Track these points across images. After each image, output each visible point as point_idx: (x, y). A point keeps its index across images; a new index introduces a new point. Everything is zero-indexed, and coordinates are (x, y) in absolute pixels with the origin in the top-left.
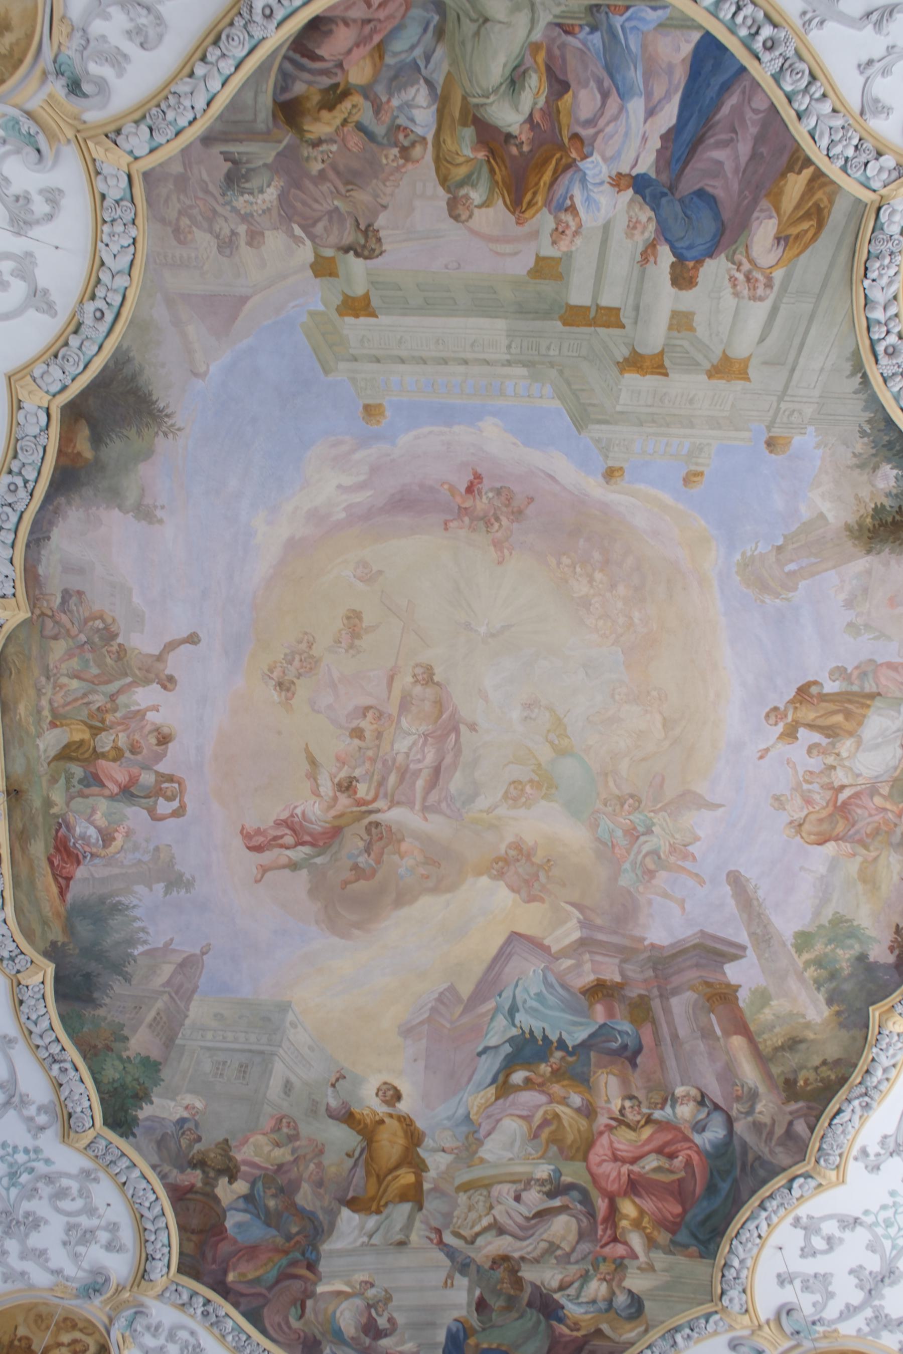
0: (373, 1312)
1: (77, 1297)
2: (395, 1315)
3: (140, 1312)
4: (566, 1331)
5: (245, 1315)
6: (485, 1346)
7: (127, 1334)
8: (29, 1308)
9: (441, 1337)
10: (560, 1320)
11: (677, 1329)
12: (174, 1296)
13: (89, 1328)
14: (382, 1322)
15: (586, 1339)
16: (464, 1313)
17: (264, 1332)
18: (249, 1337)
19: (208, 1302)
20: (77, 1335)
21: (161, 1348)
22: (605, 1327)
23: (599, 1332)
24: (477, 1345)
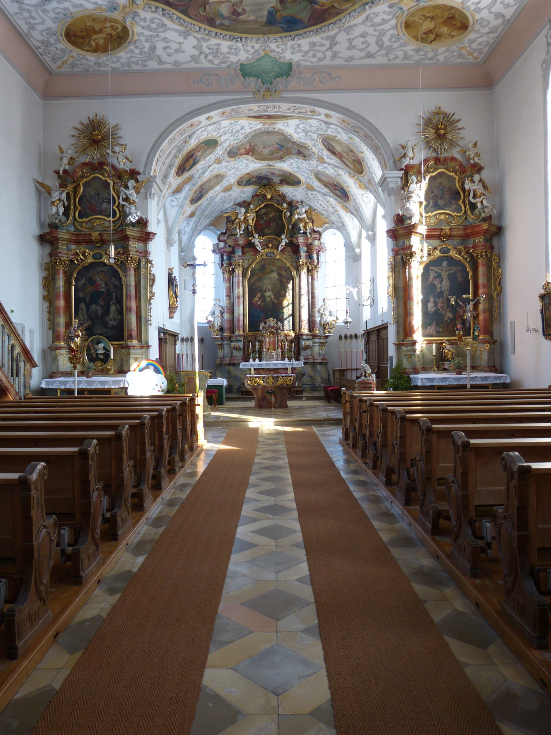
0: (235, 7)
1: (107, 11)
2: (245, 7)
3: (136, 14)
4: (319, 7)
5: (180, 12)
6: (284, 15)
7: (133, 22)
8: (89, 16)
9: (265, 13)
10: (316, 4)
11: (366, 4)
12: (149, 9)
13: (116, 21)
14: (240, 10)
15: (327, 10)
16: (274, 4)
17: (190, 17)
18: (184, 20)
19: (163, 10)
20: (113, 24)
21: (149, 26)
22: (336, 5)
23: (333, 7)
24: (281, 15)
